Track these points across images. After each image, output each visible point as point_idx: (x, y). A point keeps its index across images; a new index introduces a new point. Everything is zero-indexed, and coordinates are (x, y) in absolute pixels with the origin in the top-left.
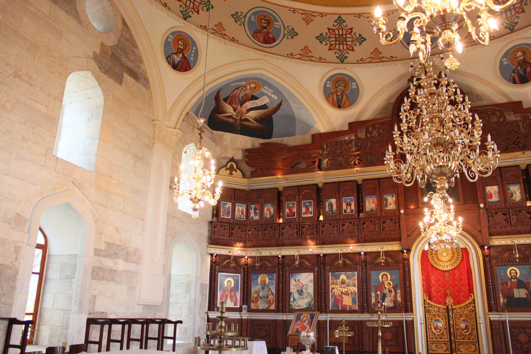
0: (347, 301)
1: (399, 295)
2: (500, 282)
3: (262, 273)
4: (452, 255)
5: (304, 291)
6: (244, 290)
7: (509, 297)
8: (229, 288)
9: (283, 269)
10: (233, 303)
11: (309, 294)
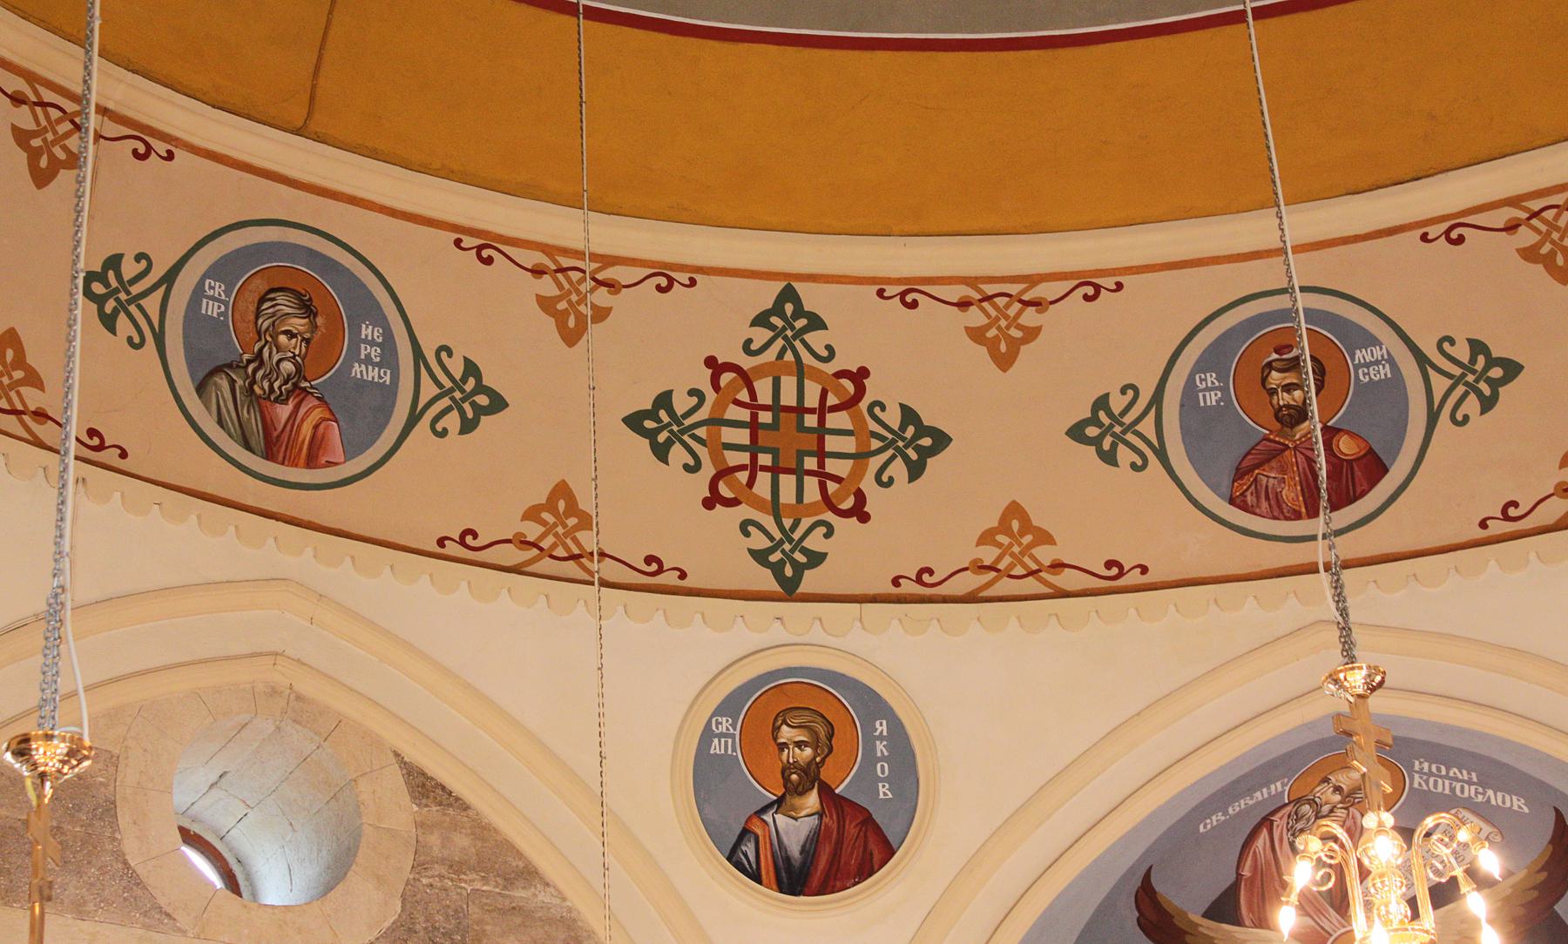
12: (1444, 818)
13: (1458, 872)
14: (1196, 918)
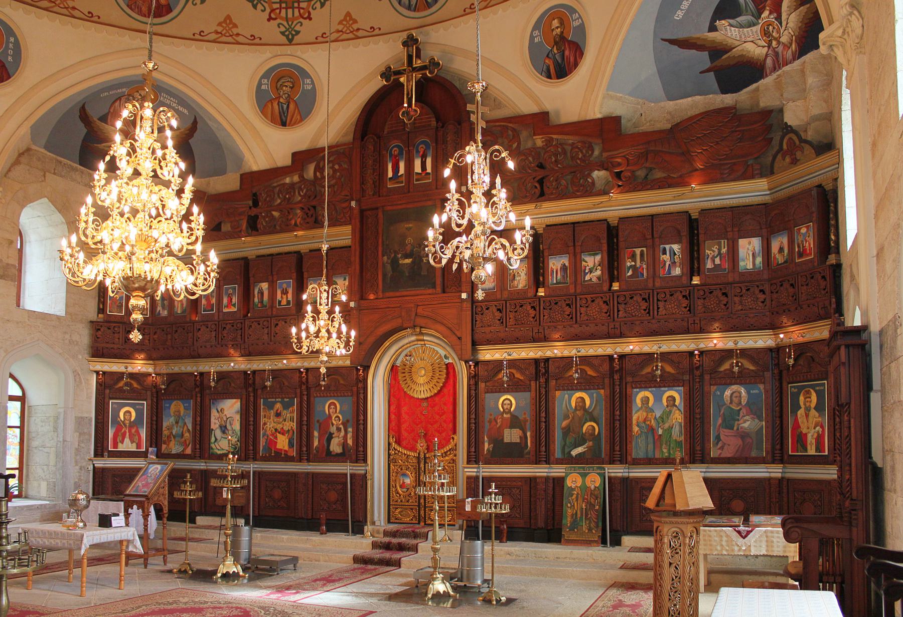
0: (282, 442)
1: (350, 435)
2: (487, 417)
3: (175, 399)
4: (431, 374)
5: (229, 427)
6: (152, 424)
7: (497, 442)
8: (127, 422)
9: (201, 393)
10: (134, 445)
11: (233, 430)
12: (165, 109)
13: (166, 124)
14: (95, 119)
